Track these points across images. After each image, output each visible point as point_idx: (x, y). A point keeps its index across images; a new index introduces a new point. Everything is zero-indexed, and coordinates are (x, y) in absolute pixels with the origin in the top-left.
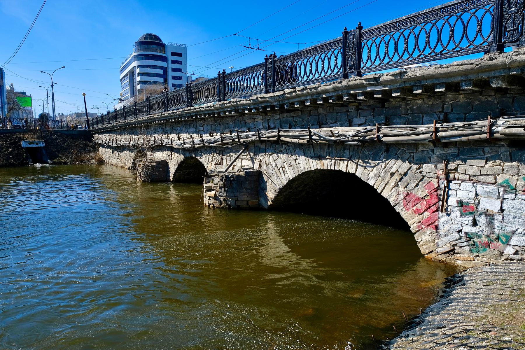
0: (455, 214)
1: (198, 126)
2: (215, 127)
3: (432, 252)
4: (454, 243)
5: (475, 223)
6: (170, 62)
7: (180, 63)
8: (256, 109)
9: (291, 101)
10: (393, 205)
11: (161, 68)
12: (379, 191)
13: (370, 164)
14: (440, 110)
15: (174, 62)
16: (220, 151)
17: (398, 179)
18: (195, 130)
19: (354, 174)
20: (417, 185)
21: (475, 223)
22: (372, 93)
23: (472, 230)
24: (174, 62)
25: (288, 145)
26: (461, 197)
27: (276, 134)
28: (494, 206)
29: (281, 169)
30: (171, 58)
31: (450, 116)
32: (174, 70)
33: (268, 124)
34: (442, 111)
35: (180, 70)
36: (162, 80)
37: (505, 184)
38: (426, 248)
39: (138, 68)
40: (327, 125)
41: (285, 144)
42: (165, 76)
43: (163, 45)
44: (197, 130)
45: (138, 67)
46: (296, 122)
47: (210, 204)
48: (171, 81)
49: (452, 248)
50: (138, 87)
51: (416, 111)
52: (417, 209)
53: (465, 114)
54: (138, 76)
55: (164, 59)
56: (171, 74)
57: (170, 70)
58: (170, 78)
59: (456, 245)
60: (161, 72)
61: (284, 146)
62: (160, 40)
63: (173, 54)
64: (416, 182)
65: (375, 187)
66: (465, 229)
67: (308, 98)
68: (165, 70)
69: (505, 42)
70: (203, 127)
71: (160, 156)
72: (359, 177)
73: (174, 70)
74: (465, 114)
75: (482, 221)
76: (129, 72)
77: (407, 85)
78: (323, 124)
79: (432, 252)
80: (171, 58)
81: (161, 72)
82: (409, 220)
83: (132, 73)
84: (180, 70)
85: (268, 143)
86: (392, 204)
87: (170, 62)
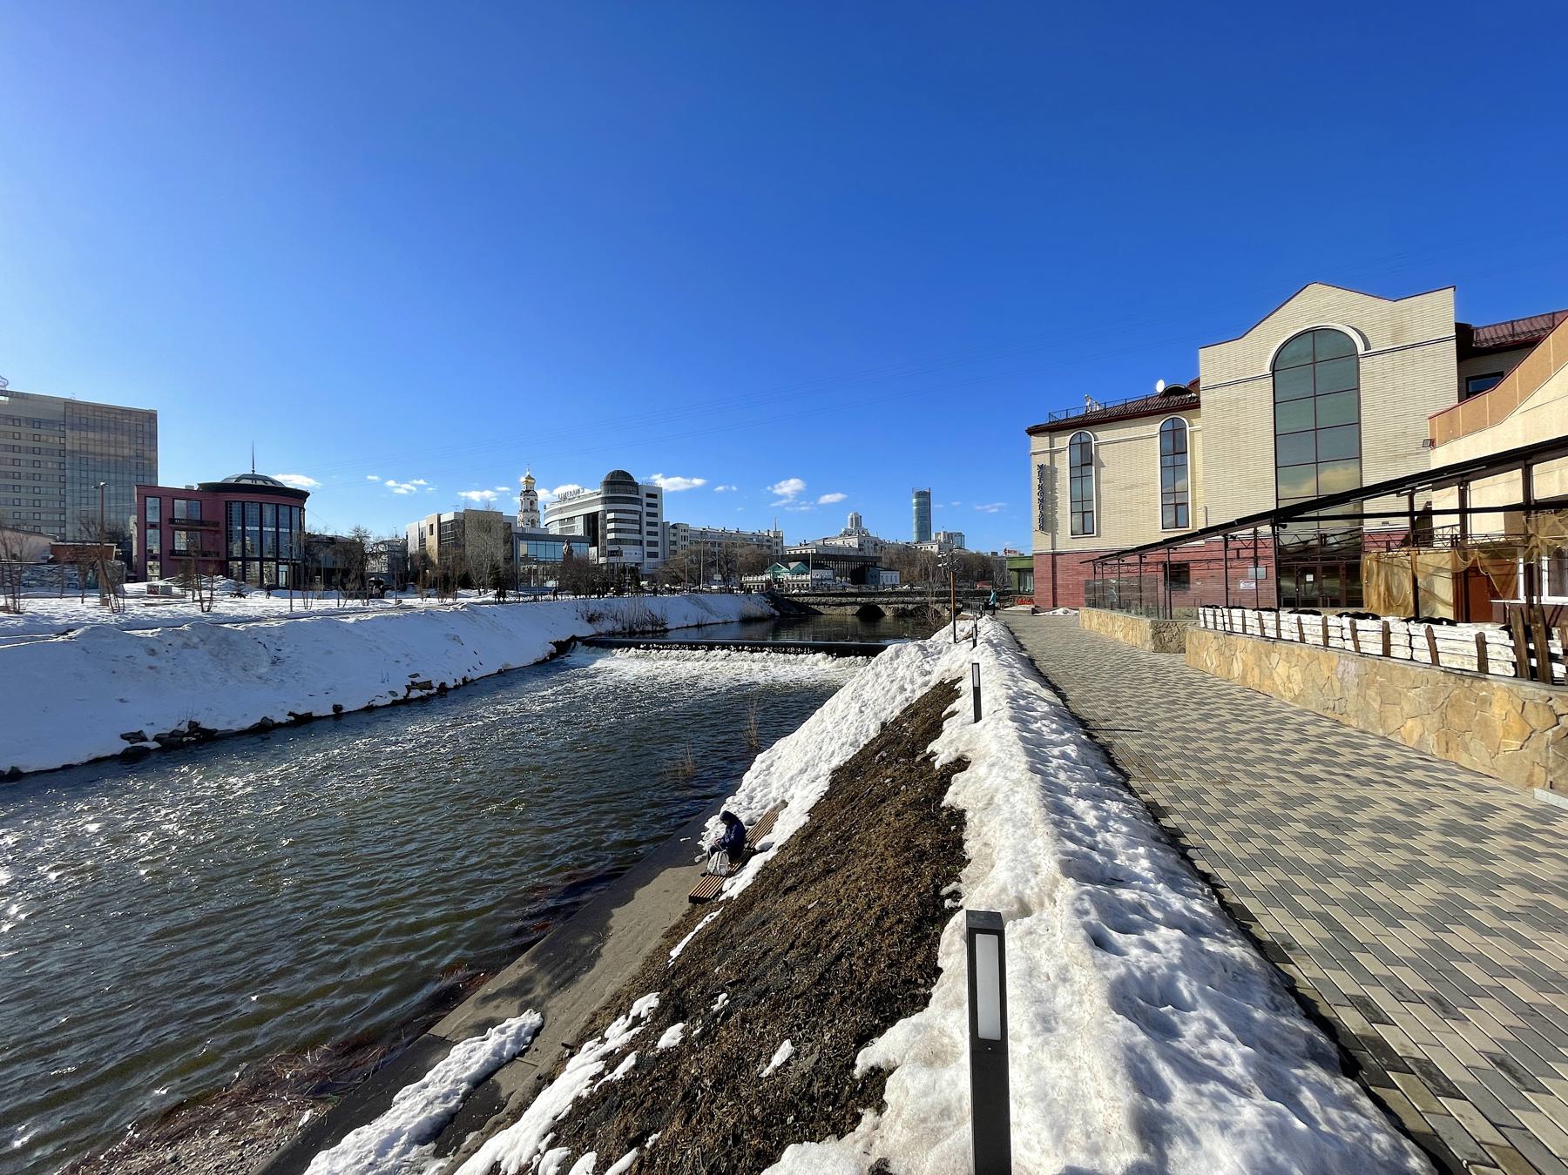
6: (644, 504)
7: (655, 506)
11: (635, 512)
13: (1175, 549)
15: (649, 505)
24: (649, 505)
30: (646, 500)
35: (655, 515)
43: (635, 485)
48: (646, 529)
56: (646, 519)
57: (644, 514)
58: (644, 524)
60: (637, 517)
62: (631, 478)
63: (649, 495)
73: (649, 514)
81: (637, 517)
84: (655, 515)
87: (644, 504)
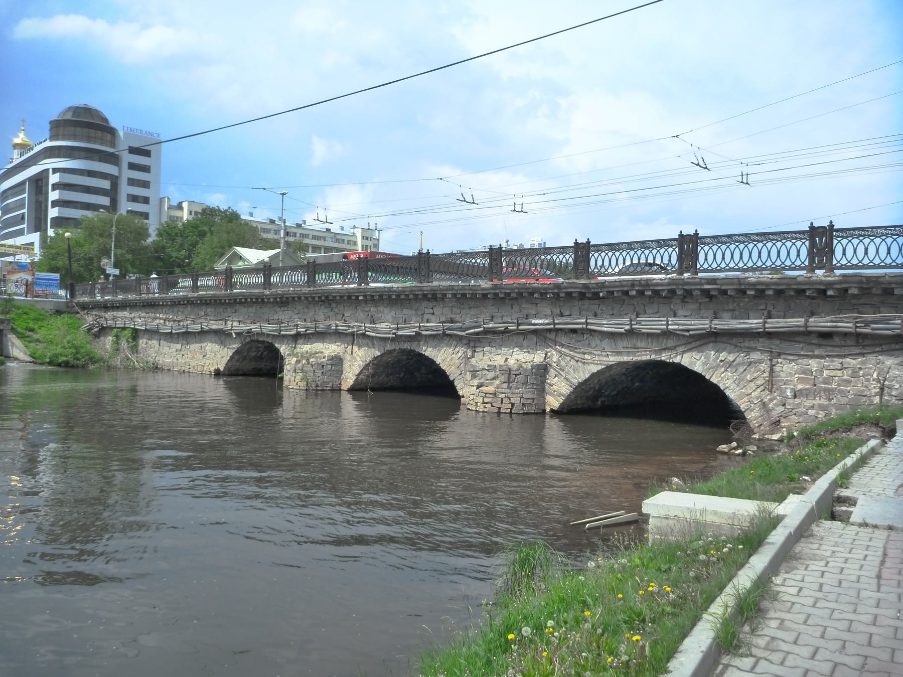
3: (761, 425)
4: (779, 415)
6: (125, 165)
8: (553, 294)
9: (611, 289)
10: (722, 389)
12: (707, 377)
14: (764, 308)
15: (132, 166)
16: (469, 341)
17: (728, 365)
20: (745, 370)
22: (708, 291)
24: (132, 166)
25: (591, 335)
27: (584, 321)
30: (127, 158)
31: (774, 312)
32: (132, 182)
33: (560, 311)
34: (765, 309)
36: (105, 201)
38: (756, 423)
40: (646, 316)
41: (588, 334)
42: (113, 193)
43: (112, 132)
45: (55, 171)
47: (486, 403)
48: (125, 206)
49: (778, 419)
50: (53, 213)
54: (53, 190)
55: (113, 159)
56: (125, 190)
59: (781, 416)
60: (106, 184)
61: (585, 336)
62: (106, 120)
63: (133, 151)
64: (745, 367)
65: (703, 374)
67: (637, 288)
68: (115, 181)
69: (816, 267)
70: (432, 308)
71: (330, 349)
72: (686, 365)
73: (132, 182)
77: (743, 287)
78: (640, 314)
79: (761, 425)
80: (127, 158)
81: (106, 184)
82: (739, 401)
83: (39, 183)
84: (145, 184)
85: (560, 332)
86: (722, 388)
87: (125, 165)
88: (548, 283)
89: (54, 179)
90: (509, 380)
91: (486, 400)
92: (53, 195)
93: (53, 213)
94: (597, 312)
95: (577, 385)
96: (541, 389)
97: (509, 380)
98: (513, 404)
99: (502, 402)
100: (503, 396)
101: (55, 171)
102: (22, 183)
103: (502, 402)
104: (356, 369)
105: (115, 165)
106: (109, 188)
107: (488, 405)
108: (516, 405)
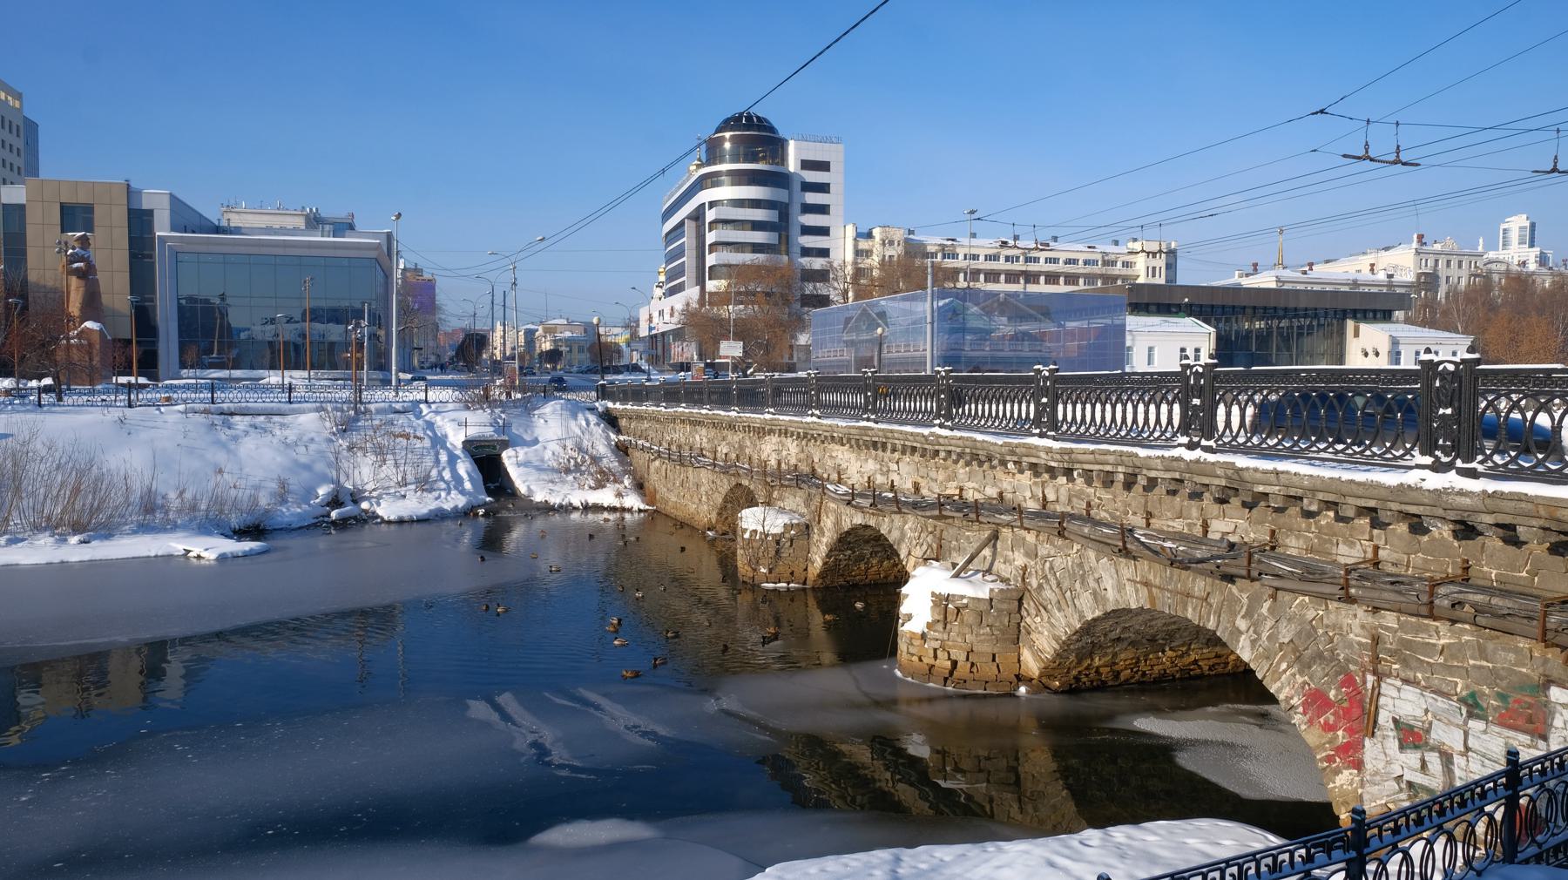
0: (1393, 745)
1: (886, 459)
2: (925, 470)
5: (1424, 765)
18: (878, 466)
19: (1214, 632)
21: (1424, 765)
23: (1418, 778)
26: (1402, 713)
28: (1453, 740)
29: (1069, 592)
33: (1043, 492)
37: (1470, 702)
39: (710, 208)
44: (885, 469)
46: (1099, 498)
51: (1326, 531)
52: (1326, 723)
53: (1409, 554)
57: (796, 208)
62: (772, 129)
63: (807, 165)
65: (1252, 666)
66: (1408, 777)
68: (783, 210)
70: (897, 463)
74: (1409, 554)
75: (1434, 760)
76: (689, 217)
87: (797, 187)
88: (1000, 442)
89: (710, 215)
90: (946, 618)
91: (912, 650)
92: (710, 238)
93: (711, 260)
94: (1092, 503)
95: (1064, 638)
96: (1016, 635)
97: (946, 618)
98: (955, 664)
99: (936, 657)
100: (937, 644)
101: (712, 204)
102: (681, 224)
103: (936, 657)
104: (824, 549)
105: (784, 188)
106: (776, 220)
107: (915, 659)
108: (959, 664)
